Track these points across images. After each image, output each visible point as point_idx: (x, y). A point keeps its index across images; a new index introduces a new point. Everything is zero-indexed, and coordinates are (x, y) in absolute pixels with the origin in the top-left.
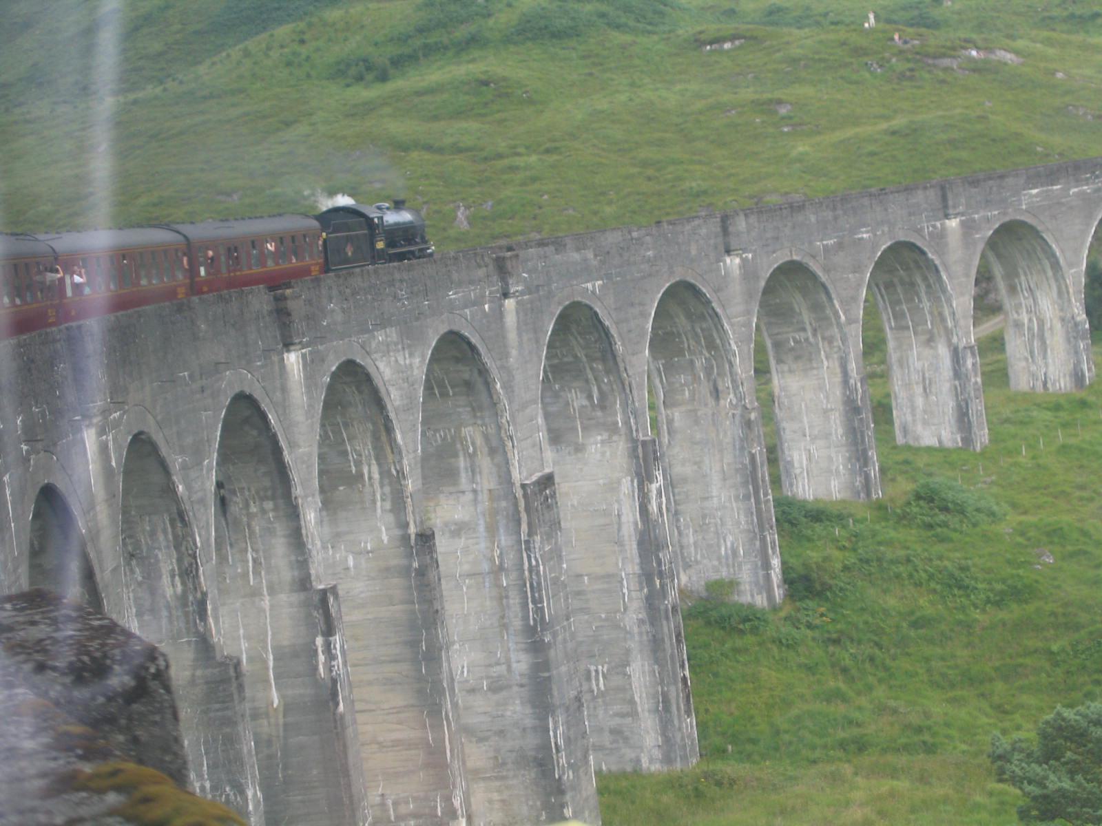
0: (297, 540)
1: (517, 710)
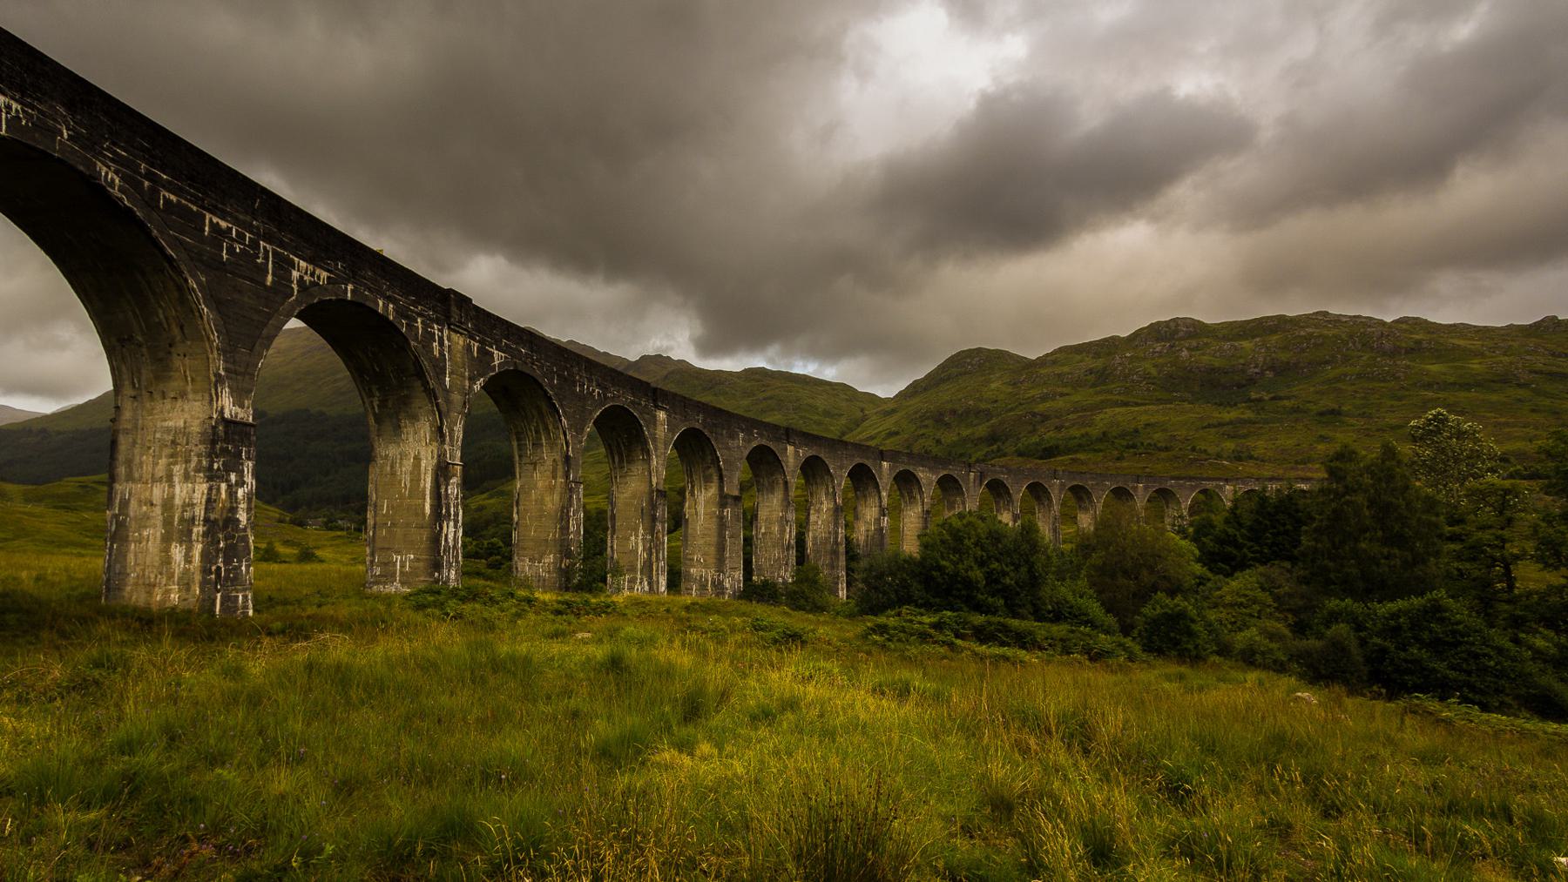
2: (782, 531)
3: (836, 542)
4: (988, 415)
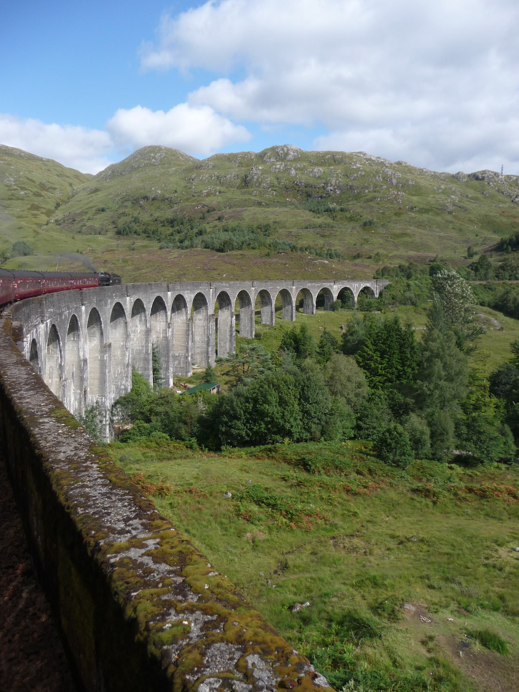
0: (166, 316)
1: (205, 346)
2: (124, 355)
3: (147, 353)
4: (171, 202)
